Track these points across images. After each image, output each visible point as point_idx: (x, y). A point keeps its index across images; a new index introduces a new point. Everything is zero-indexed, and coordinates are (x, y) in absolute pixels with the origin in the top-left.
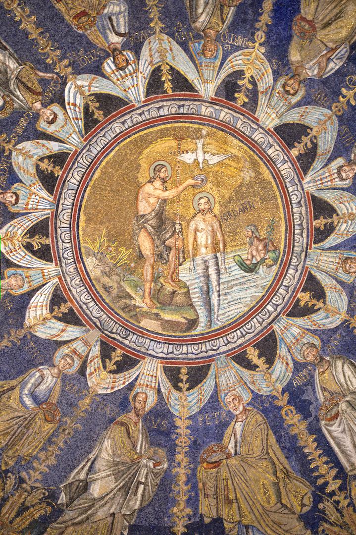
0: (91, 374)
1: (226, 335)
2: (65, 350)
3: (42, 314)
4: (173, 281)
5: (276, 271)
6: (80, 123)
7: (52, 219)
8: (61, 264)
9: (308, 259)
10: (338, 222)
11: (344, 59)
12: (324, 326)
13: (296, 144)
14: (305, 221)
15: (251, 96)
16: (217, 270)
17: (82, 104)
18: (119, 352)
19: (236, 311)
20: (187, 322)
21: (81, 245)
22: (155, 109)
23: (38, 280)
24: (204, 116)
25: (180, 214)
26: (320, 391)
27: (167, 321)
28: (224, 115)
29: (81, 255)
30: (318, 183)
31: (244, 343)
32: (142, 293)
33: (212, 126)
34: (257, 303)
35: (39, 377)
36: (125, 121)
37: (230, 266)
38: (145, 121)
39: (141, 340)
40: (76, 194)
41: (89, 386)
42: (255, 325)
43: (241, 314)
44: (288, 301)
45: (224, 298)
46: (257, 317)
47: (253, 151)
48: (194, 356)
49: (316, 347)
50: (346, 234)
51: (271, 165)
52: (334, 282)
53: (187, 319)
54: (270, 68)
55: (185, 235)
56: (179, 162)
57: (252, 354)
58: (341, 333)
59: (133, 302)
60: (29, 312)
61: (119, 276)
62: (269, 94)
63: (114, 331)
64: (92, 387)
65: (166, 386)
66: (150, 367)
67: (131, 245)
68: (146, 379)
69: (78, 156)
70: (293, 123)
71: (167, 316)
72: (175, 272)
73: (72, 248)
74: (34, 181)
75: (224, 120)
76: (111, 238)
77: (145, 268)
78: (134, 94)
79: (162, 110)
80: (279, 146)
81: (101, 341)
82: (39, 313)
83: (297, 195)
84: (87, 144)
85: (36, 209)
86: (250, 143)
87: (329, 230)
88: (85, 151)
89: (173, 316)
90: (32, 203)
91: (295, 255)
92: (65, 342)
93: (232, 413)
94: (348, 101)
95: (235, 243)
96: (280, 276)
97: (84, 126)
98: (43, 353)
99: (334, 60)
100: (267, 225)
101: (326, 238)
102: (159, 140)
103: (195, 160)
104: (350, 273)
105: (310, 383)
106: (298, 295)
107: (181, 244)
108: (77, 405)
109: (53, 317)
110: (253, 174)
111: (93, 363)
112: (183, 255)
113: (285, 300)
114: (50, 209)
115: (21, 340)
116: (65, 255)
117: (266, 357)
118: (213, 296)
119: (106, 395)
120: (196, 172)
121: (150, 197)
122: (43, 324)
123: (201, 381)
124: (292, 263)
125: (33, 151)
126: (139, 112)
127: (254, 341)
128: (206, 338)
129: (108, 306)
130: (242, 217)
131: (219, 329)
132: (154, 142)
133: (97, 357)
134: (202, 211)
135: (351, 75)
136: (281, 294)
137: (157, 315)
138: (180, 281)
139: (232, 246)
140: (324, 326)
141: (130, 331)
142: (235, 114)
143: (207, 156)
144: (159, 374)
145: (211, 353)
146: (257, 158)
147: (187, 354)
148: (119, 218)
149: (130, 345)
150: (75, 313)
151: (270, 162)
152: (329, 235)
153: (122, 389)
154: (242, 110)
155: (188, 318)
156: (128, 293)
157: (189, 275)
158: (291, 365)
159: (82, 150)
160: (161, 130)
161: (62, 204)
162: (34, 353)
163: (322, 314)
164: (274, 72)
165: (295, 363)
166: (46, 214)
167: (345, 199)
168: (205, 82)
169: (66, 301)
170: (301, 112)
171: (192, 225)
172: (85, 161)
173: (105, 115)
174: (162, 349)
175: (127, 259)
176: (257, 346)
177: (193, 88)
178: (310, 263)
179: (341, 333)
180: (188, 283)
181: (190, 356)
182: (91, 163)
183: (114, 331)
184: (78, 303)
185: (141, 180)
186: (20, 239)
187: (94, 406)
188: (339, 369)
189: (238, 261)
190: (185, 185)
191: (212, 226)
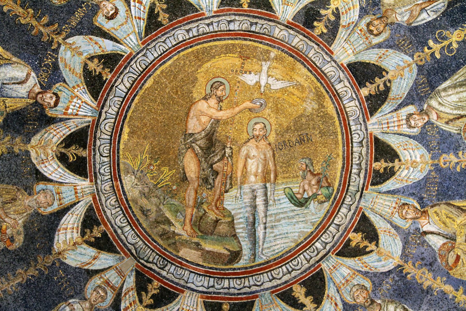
1: (271, 271)
2: (97, 281)
3: (73, 238)
4: (217, 208)
5: (328, 208)
6: (142, 23)
7: (92, 128)
9: (363, 200)
10: (400, 168)
11: (439, 14)
12: (376, 268)
13: (368, 84)
14: (364, 161)
15: (331, 27)
17: (148, 4)
18: (156, 284)
19: (282, 245)
20: (229, 253)
21: (121, 161)
22: (225, 22)
23: (70, 198)
24: (276, 38)
25: (232, 137)
27: (208, 252)
28: (297, 41)
29: (119, 172)
30: (384, 126)
31: (290, 279)
33: (282, 51)
34: (305, 239)
36: (190, 29)
37: (279, 198)
38: (211, 32)
39: (180, 271)
40: (122, 103)
42: (302, 262)
43: (287, 249)
44: (338, 240)
45: (271, 231)
46: (305, 254)
47: (321, 83)
48: (236, 292)
49: (366, 289)
50: (406, 181)
51: (337, 100)
53: (229, 250)
54: (358, 4)
56: (239, 82)
57: (299, 292)
58: (394, 277)
59: (172, 229)
61: (159, 198)
62: (351, 29)
63: (151, 260)
66: (189, 301)
67: (175, 165)
69: (132, 60)
71: (208, 247)
72: (220, 199)
73: (110, 164)
74: (79, 83)
75: (296, 46)
76: (154, 155)
77: (188, 191)
79: (232, 24)
80: (349, 83)
81: (137, 271)
82: (69, 236)
83: (359, 135)
84: (144, 48)
85: (77, 115)
86: (319, 74)
88: (140, 55)
89: (215, 247)
90: (73, 107)
91: (349, 194)
92: (97, 272)
94: (433, 55)
95: (288, 175)
96: (331, 215)
98: (73, 284)
99: (428, 11)
100: (323, 160)
101: (384, 181)
102: (222, 55)
103: (257, 82)
104: (406, 219)
106: (350, 235)
109: (84, 241)
110: (316, 106)
111: (127, 296)
112: (230, 182)
113: (335, 239)
114: (92, 116)
116: (102, 171)
117: (313, 296)
118: (259, 228)
120: (256, 95)
121: (202, 115)
122: (73, 250)
124: (345, 202)
126: (207, 21)
127: (301, 278)
128: (250, 272)
129: (145, 232)
130: (298, 149)
131: (263, 264)
133: (132, 289)
136: (331, 232)
137: (198, 244)
138: (224, 209)
139: (284, 178)
140: (376, 268)
141: (168, 261)
142: (309, 42)
143: (271, 80)
145: (254, 289)
146: (324, 91)
147: (229, 289)
148: (165, 134)
149: (167, 276)
151: (336, 97)
152: (388, 179)
154: (318, 40)
155: (231, 249)
156: (168, 218)
157: (235, 203)
158: (340, 306)
159: (138, 54)
160: (227, 45)
161: (106, 112)
162: (62, 284)
164: (362, 8)
165: (345, 304)
166: (86, 122)
168: (285, 4)
169: (100, 224)
170: (380, 54)
171: (244, 151)
172: (138, 66)
175: (169, 181)
176: (304, 284)
177: (271, 7)
178: (364, 204)
179: (394, 277)
180: (233, 213)
181: (232, 291)
182: (144, 70)
183: (151, 260)
184: (112, 226)
185: (195, 95)
186: (55, 148)
189: (289, 193)
190: (242, 107)
191: (265, 155)
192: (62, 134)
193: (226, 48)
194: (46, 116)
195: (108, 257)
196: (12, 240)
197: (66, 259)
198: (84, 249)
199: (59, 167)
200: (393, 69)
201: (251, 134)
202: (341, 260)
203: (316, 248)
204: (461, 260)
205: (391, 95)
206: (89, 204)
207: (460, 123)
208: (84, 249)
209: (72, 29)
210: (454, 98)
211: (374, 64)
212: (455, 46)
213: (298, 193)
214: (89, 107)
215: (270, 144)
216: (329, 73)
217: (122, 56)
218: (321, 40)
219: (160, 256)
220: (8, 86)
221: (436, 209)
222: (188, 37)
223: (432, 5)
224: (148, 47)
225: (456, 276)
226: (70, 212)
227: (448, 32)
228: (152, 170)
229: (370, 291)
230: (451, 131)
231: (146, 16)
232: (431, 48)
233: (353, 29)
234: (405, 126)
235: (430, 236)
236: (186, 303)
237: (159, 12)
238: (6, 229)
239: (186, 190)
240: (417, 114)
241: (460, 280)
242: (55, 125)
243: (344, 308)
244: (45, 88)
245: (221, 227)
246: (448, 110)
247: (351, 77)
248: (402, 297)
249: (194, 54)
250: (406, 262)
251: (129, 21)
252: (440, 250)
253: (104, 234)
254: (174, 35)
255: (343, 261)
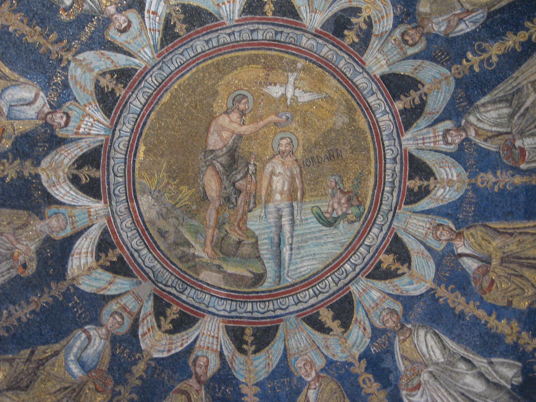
0: (144, 334)
1: (296, 294)
2: (113, 306)
3: (87, 262)
4: (240, 229)
5: (358, 228)
6: (157, 35)
7: (106, 147)
8: (110, 203)
10: (435, 187)
11: (478, 25)
12: (407, 292)
13: (402, 97)
16: (291, 220)
17: (164, 15)
18: (175, 308)
21: (137, 180)
23: (83, 221)
24: (304, 48)
26: (400, 360)
27: (230, 275)
28: (326, 50)
29: (135, 192)
30: (419, 142)
31: (317, 303)
32: (203, 240)
33: (310, 61)
34: (334, 261)
35: (85, 339)
36: (210, 39)
39: (200, 295)
40: (137, 119)
41: (143, 348)
42: (329, 285)
43: (315, 271)
44: (368, 262)
46: (333, 276)
47: (353, 96)
48: (260, 316)
49: (397, 314)
50: (442, 200)
51: (369, 113)
52: (422, 247)
54: (392, 12)
55: (258, 178)
57: (326, 316)
59: (192, 251)
60: (72, 260)
61: (178, 219)
64: (145, 350)
65: (229, 349)
67: (195, 183)
68: (207, 340)
69: (147, 74)
70: (404, 75)
71: (230, 269)
72: (243, 219)
74: (91, 100)
75: (326, 56)
76: (172, 174)
77: (209, 211)
78: (228, 10)
79: (256, 33)
80: (383, 95)
83: (393, 151)
87: (424, 192)
88: (156, 68)
90: (84, 126)
91: (381, 213)
92: (113, 297)
93: (304, 380)
94: (471, 67)
95: (316, 193)
97: (162, 39)
99: (467, 22)
101: (419, 200)
103: (283, 94)
104: (440, 240)
105: (390, 351)
106: (381, 257)
107: (253, 187)
108: (130, 371)
110: (347, 120)
111: (145, 321)
112: (254, 200)
113: (366, 260)
115: (63, 294)
116: (117, 192)
117: (340, 320)
119: (163, 359)
121: (225, 129)
122: (87, 275)
123: (268, 344)
124: (377, 222)
125: (95, 63)
126: (228, 31)
129: (164, 255)
132: (239, 69)
133: (150, 314)
134: (282, 153)
135: (482, 41)
137: (219, 267)
138: (247, 229)
139: (312, 196)
141: (187, 284)
142: (339, 52)
143: (298, 93)
144: (221, 334)
145: (279, 312)
150: (125, 262)
151: (369, 110)
153: (180, 352)
154: (349, 50)
155: (254, 271)
156: (187, 240)
157: (259, 223)
158: (369, 330)
159: (153, 67)
161: (119, 130)
163: (406, 279)
164: (396, 17)
167: (447, 164)
168: (313, 11)
171: (269, 168)
172: (154, 80)
173: (188, 30)
174: (224, 306)
175: (188, 200)
176: (331, 307)
177: (298, 15)
179: (425, 302)
180: (257, 233)
181: (256, 315)
182: (160, 84)
184: (128, 250)
186: (66, 170)
187: (149, 372)
188: (422, 338)
190: (266, 121)
191: (291, 172)
192: (73, 155)
193: (249, 59)
194: (56, 137)
195: (124, 282)
196: (24, 266)
197: (80, 284)
198: (100, 274)
199: (71, 189)
200: (429, 81)
201: (276, 150)
202: (371, 283)
203: (345, 270)
204: (495, 285)
205: (427, 109)
206: (103, 227)
207: (499, 141)
208: (100, 274)
209: (81, 44)
210: (493, 114)
211: (409, 76)
212: (495, 59)
213: (327, 212)
214: (101, 125)
215: (296, 160)
216: (361, 85)
217: (136, 70)
218: (352, 49)
219: (179, 279)
220: (16, 108)
221: (472, 231)
222: (207, 48)
223: (471, 16)
224: (164, 60)
225: (489, 301)
226: (83, 236)
227: (487, 44)
228: (170, 190)
229: (401, 315)
230: (490, 149)
231: (161, 27)
232: (470, 61)
233: (386, 39)
234: (441, 142)
235: (465, 259)
236: (206, 328)
237: (175, 23)
238: (18, 256)
239: (207, 209)
240: (455, 131)
241: (494, 306)
242: (66, 145)
243: (373, 333)
244: (55, 108)
245: (243, 249)
246: (487, 127)
247: (384, 89)
248: (433, 322)
249: (214, 65)
250: (439, 285)
251: (143, 33)
252: (474, 273)
253: (120, 258)
254: (192, 46)
255: (374, 284)
